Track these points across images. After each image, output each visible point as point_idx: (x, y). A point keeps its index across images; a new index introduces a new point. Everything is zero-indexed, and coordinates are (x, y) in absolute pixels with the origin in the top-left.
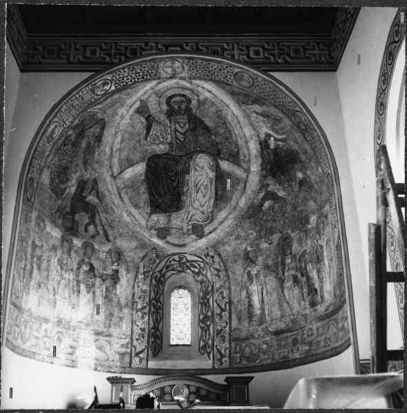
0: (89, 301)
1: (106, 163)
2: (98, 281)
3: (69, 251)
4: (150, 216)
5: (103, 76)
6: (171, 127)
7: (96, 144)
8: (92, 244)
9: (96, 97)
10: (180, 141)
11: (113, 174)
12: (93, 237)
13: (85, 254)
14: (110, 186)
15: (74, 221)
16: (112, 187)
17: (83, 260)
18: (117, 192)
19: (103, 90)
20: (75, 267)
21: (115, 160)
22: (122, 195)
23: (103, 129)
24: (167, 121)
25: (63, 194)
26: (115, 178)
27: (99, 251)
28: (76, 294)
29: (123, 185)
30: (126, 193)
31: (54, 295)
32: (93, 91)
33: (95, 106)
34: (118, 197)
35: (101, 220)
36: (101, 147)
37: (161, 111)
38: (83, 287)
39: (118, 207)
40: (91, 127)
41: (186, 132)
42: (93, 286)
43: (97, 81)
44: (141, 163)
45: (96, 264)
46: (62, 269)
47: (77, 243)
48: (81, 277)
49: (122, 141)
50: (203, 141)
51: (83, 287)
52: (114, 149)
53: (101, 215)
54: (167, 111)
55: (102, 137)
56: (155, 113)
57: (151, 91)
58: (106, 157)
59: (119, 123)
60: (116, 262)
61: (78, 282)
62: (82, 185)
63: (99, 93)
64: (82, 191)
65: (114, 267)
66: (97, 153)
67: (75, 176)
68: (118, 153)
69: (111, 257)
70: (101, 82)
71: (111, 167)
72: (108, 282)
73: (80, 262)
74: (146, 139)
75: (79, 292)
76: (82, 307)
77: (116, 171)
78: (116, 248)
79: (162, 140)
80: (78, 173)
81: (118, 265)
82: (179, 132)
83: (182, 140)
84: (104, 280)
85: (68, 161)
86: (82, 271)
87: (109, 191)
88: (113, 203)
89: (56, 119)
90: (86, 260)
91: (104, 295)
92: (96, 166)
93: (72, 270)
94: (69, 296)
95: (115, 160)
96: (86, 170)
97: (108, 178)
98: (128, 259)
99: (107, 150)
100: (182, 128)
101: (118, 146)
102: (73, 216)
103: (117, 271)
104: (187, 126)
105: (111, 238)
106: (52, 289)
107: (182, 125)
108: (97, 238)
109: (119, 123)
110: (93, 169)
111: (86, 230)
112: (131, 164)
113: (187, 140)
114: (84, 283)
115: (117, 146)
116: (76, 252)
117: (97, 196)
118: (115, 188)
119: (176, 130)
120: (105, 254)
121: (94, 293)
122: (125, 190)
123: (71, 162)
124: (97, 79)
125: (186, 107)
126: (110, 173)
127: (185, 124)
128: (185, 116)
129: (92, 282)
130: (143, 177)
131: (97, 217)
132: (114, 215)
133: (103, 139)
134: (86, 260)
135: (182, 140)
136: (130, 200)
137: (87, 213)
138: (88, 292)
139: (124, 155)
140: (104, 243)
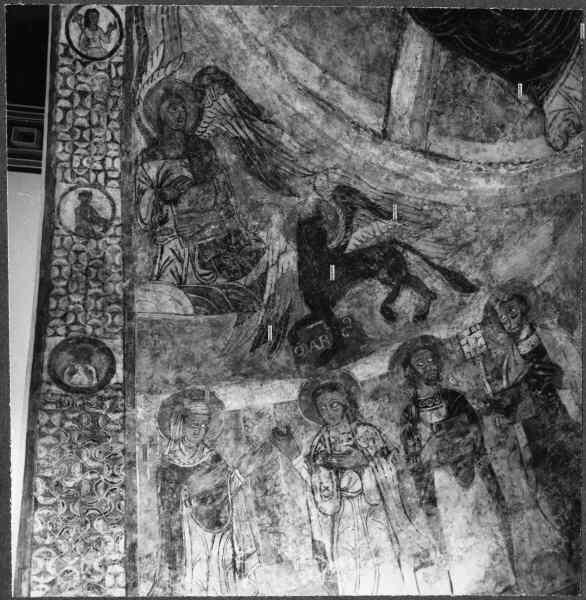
0: (478, 510)
1: (334, 130)
2: (490, 425)
3: (351, 412)
4: (543, 113)
5: (57, 18)
7: (259, 123)
8: (425, 338)
9: (117, 59)
11: (375, 134)
12: (421, 316)
13: (413, 381)
14: (392, 165)
15: (336, 325)
16: (400, 160)
17: (416, 400)
18: (419, 159)
19: (108, 34)
20: (393, 435)
21: (348, 102)
22: (437, 149)
23: (228, 83)
25: (263, 291)
26: (385, 135)
27: (458, 337)
28: (420, 517)
29: (416, 126)
30: (442, 133)
31: (321, 566)
32: (87, 60)
33: (142, 70)
34: (432, 165)
35: (426, 259)
36: (280, 117)
38: (442, 478)
39: (448, 187)
40: (200, 113)
42: (479, 452)
43: (63, 38)
44: (406, 35)
45: (459, 380)
46: (339, 471)
47: (369, 370)
48: (428, 454)
49: (308, 53)
51: (442, 478)
52: (315, 87)
53: (420, 245)
55: (249, 101)
58: (318, 121)
59: (246, 36)
60: (521, 326)
61: (422, 475)
62: (309, 234)
63: (110, 47)
64: (322, 238)
65: (524, 348)
66: (285, 138)
67: (274, 231)
68: (334, 84)
69: (502, 325)
70: (73, 26)
71: (357, 127)
72: (526, 408)
73: (406, 410)
75: (433, 501)
76: (455, 543)
77: (370, 118)
78: (502, 288)
80: (276, 218)
81: (533, 330)
84: (508, 412)
85: (222, 222)
86: (425, 432)
87: (398, 176)
88: (430, 188)
89: (62, 187)
90: (425, 391)
91: (528, 456)
92: (316, 160)
93: (385, 453)
94: (394, 538)
95: (348, 102)
96: (292, 193)
97: (372, 152)
98: (551, 289)
99: (301, 106)
101: (317, 71)
102: (329, 316)
103: (539, 352)
105: (473, 276)
106: (306, 552)
108: (435, 312)
109: (246, 36)
110: (314, 174)
111: (390, 315)
112: (387, 65)
114: (441, 465)
115: (311, 78)
116: (374, 396)
117: (378, 212)
118: (403, 154)
120: (478, 334)
121: (489, 472)
122: (432, 129)
123: (230, 215)
124: (56, 33)
126: (367, 137)
129: (472, 442)
130: (444, 55)
131: (411, 257)
132: (453, 214)
133: (257, 101)
134: (425, 391)
136: (465, 137)
137: (372, 275)
138: (466, 482)
139: (351, 70)
140: (463, 304)
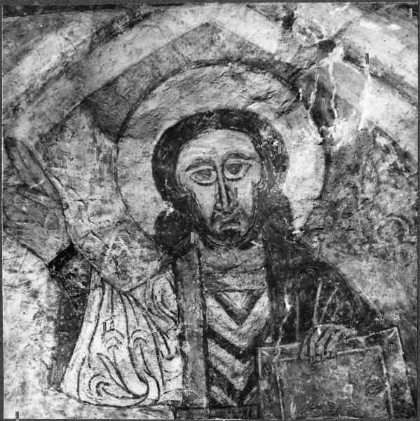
6: (180, 315)
10: (230, 389)
24: (163, 284)
37: (128, 225)
41: (257, 342)
50: (348, 389)
54: (160, 220)
56: (101, 233)
57: (65, 86)
74: (55, 382)
79: (139, 388)
82: (225, 344)
83: (239, 384)
100: (239, 318)
104: (263, 307)
107: (239, 303)
113: (264, 385)
119: (209, 333)
125: (260, 197)
127: (254, 298)
128: (255, 255)
135: (239, 384)
